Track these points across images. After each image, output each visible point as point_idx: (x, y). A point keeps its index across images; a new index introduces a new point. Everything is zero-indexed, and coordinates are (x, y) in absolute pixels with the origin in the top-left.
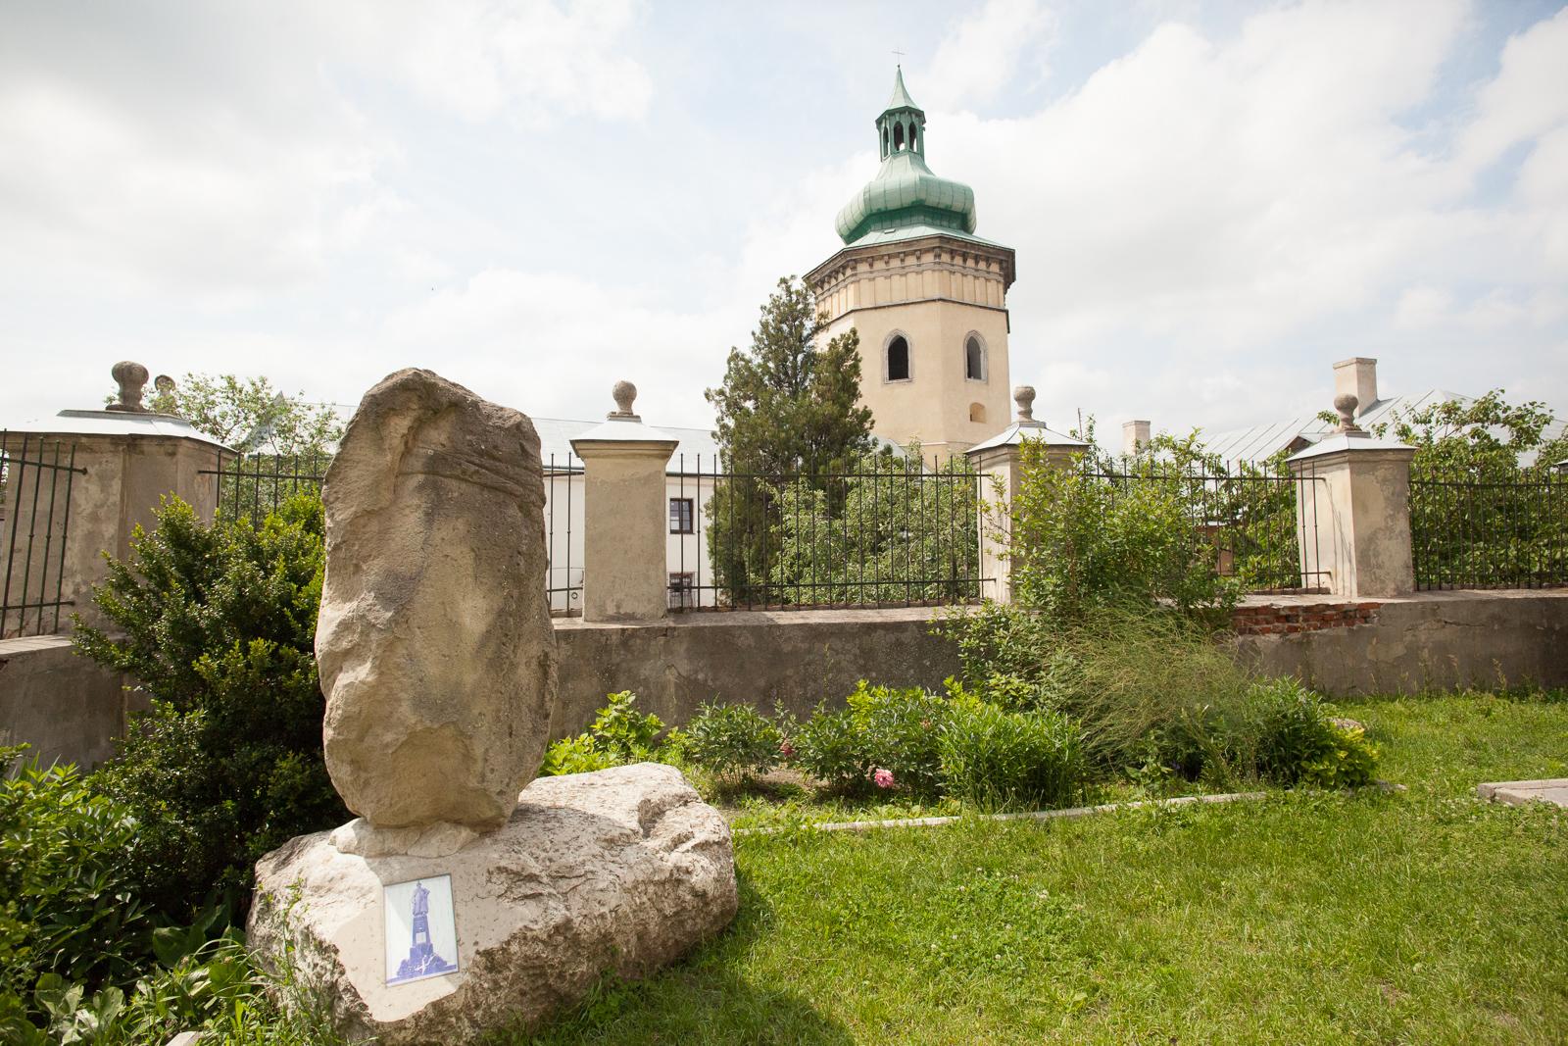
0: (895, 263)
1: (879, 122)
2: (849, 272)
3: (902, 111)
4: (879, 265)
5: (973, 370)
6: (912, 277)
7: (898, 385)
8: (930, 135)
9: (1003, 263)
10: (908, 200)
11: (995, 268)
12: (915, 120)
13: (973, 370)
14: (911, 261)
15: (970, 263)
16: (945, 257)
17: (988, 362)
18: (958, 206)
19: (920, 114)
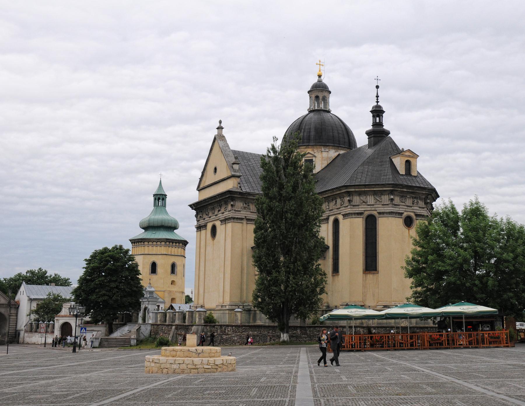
0: (155, 243)
1: (154, 195)
2: (142, 243)
3: (160, 195)
4: (150, 243)
5: (173, 271)
6: (158, 247)
7: (154, 276)
8: (168, 200)
9: (185, 243)
10: (159, 224)
11: (181, 245)
12: (164, 197)
13: (173, 271)
14: (159, 243)
15: (174, 244)
16: (168, 243)
17: (178, 269)
18: (173, 226)
19: (166, 195)
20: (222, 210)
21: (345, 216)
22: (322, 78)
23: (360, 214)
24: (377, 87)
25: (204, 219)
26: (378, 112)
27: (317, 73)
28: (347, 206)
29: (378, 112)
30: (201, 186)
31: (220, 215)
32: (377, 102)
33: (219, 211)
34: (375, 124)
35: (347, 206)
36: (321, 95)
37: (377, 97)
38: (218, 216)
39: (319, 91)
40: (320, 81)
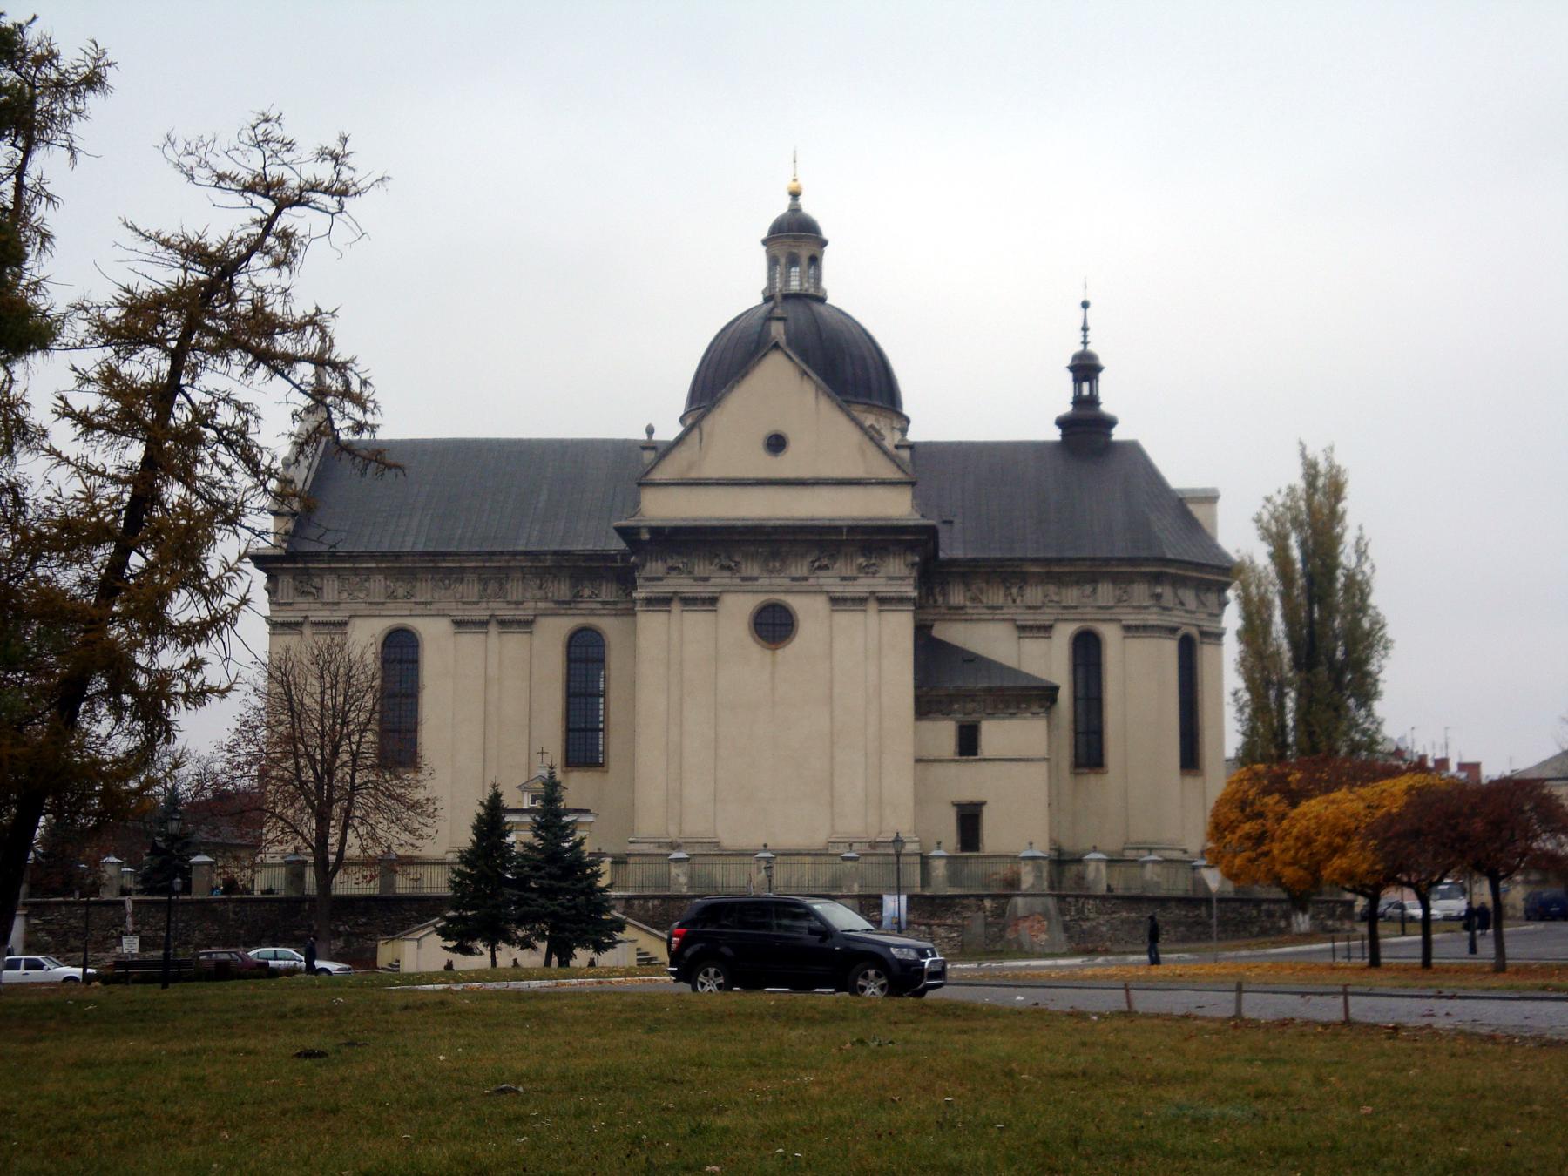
20: (842, 567)
21: (1130, 630)
22: (802, 200)
23: (1173, 630)
24: (1085, 305)
25: (707, 579)
26: (1085, 368)
27: (788, 184)
28: (1146, 608)
29: (1085, 368)
30: (657, 475)
31: (822, 581)
32: (1085, 343)
33: (826, 567)
34: (1079, 401)
35: (1146, 608)
36: (804, 253)
37: (1085, 329)
38: (812, 581)
39: (795, 239)
40: (795, 210)
